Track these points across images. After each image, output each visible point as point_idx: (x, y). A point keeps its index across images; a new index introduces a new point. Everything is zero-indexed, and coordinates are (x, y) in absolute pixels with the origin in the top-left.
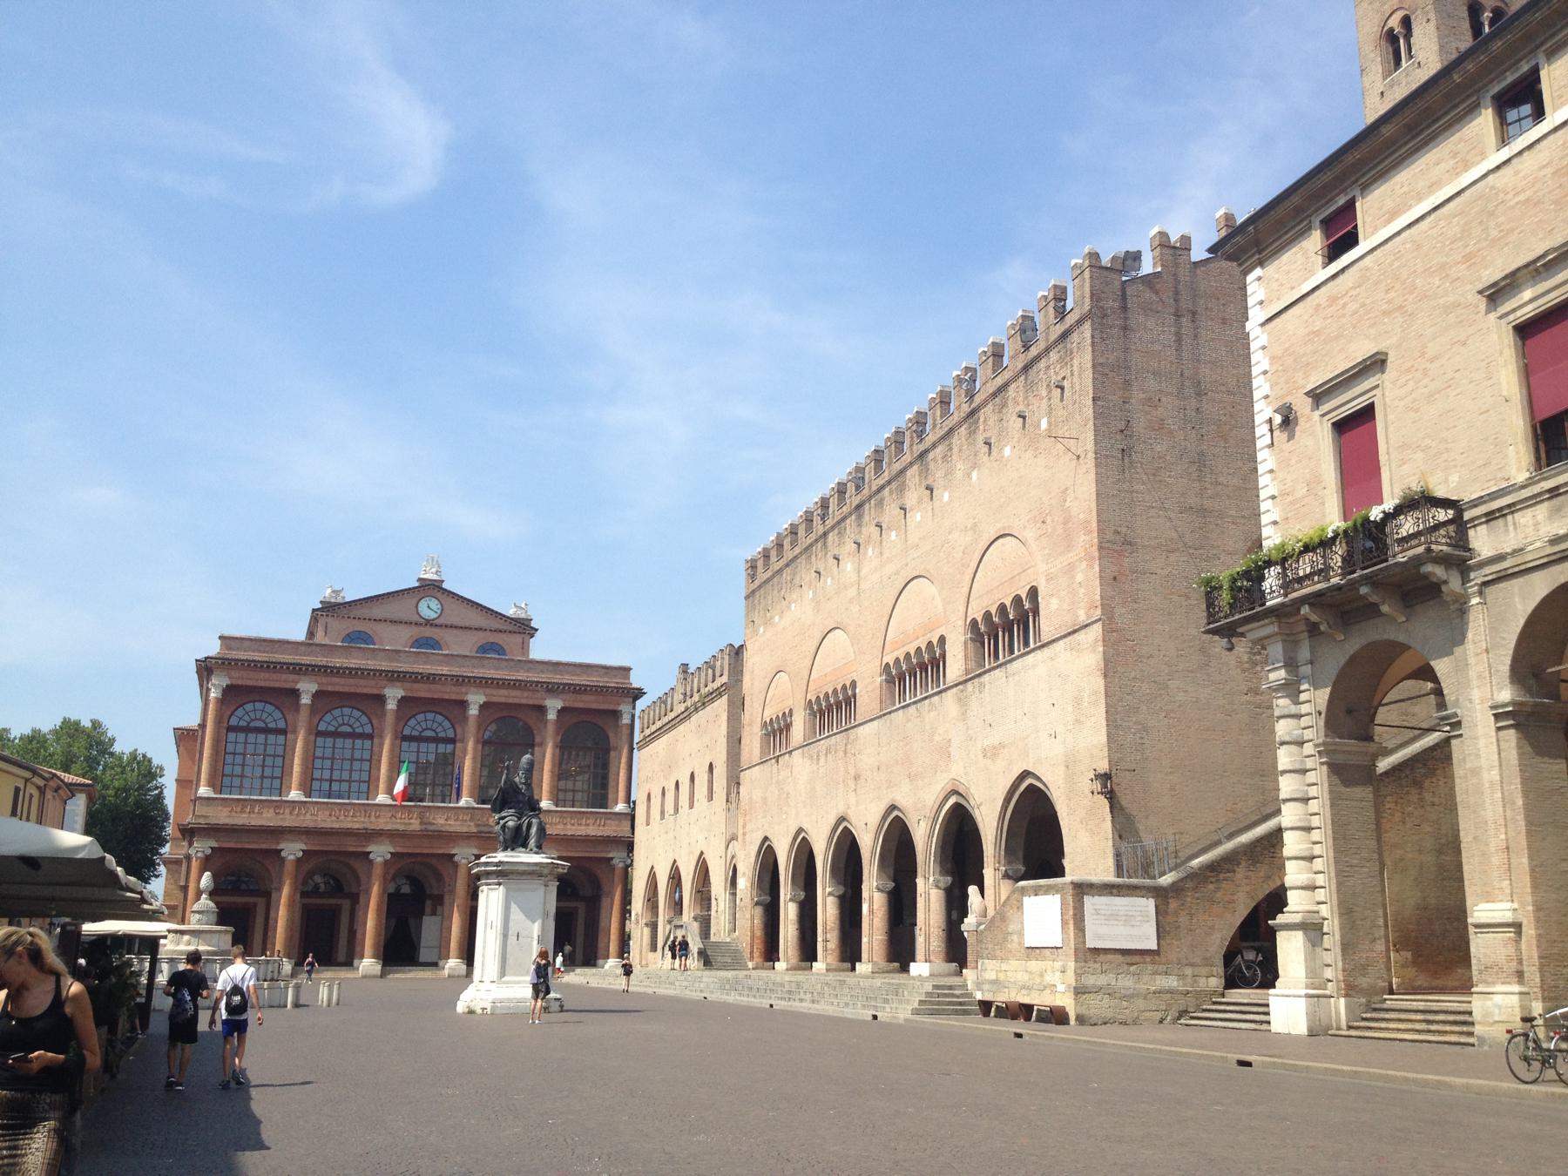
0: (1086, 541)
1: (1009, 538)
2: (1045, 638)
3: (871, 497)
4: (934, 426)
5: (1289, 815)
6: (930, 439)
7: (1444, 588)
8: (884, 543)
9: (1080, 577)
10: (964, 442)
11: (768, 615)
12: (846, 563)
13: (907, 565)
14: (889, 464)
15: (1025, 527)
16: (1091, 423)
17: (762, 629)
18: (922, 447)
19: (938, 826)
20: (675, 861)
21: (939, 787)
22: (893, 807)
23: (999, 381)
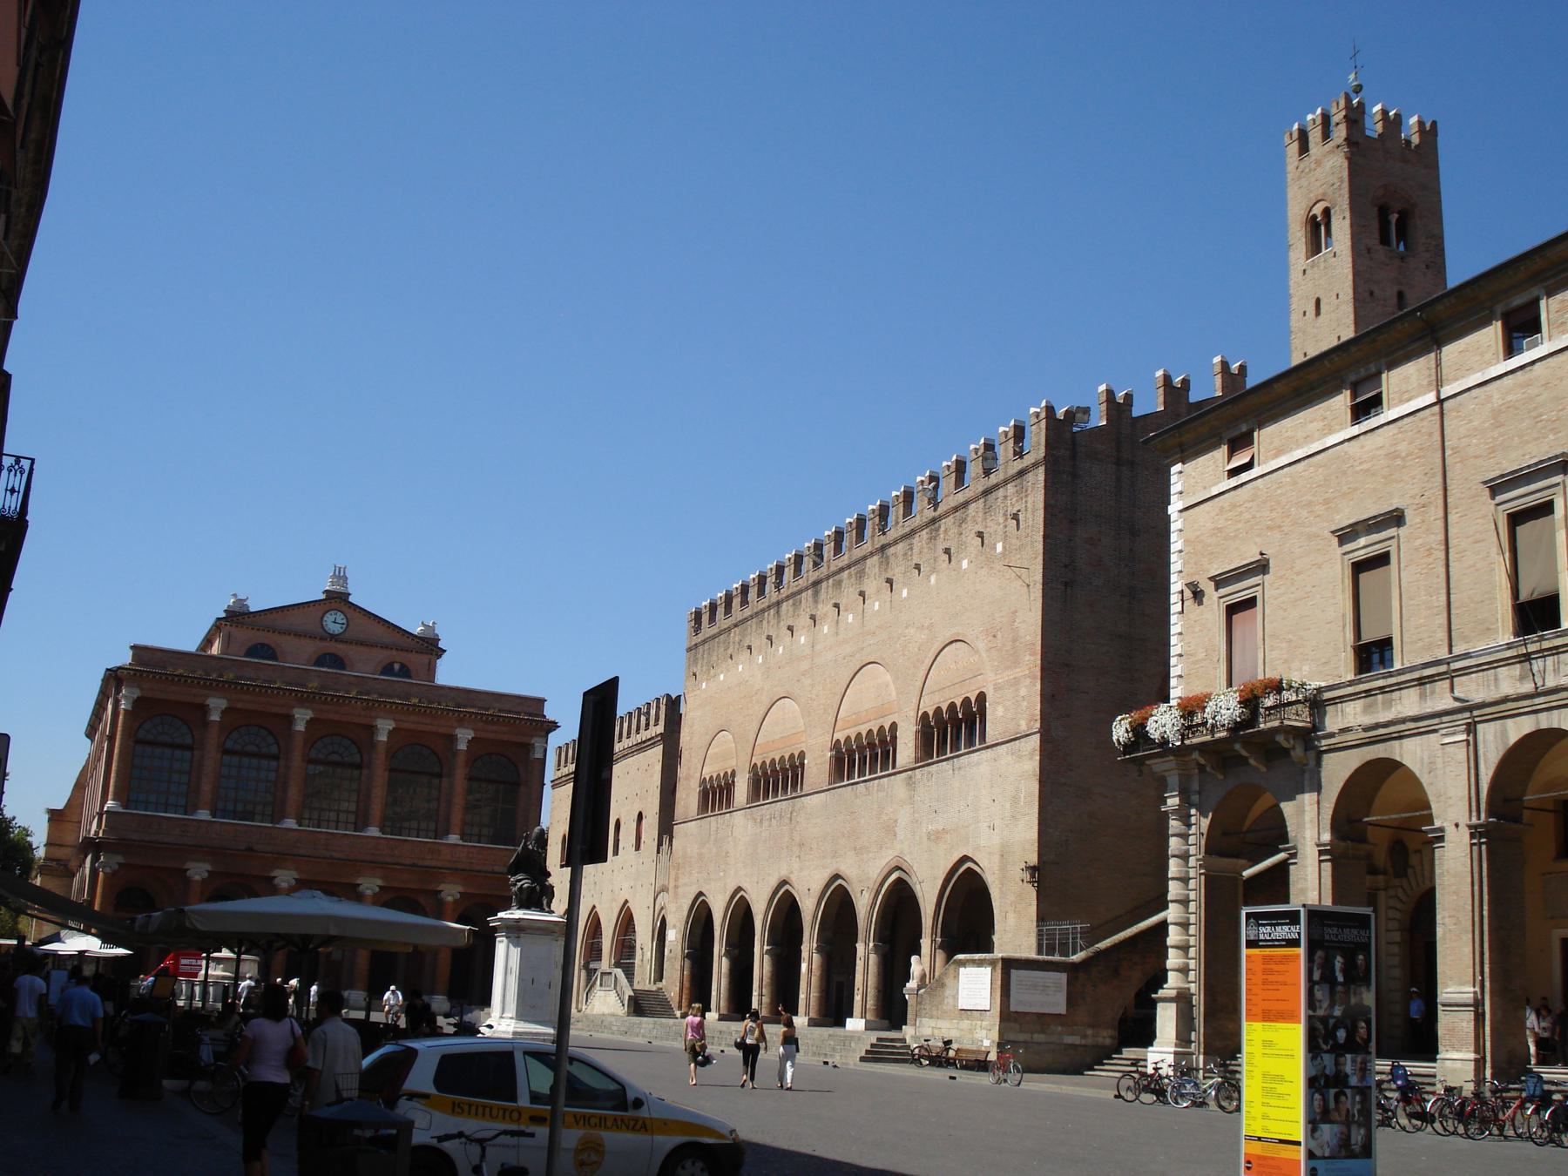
0: (1031, 661)
1: (959, 643)
2: (989, 741)
3: (828, 577)
4: (897, 523)
5: (1172, 913)
6: (892, 534)
7: (1292, 753)
8: (841, 624)
9: (1023, 692)
10: (925, 545)
11: (712, 671)
12: (800, 636)
13: (862, 649)
14: (850, 549)
15: (977, 638)
16: (1040, 558)
17: (704, 684)
18: (883, 540)
19: (880, 897)
20: (594, 907)
21: (884, 862)
22: (837, 876)
23: (961, 497)
